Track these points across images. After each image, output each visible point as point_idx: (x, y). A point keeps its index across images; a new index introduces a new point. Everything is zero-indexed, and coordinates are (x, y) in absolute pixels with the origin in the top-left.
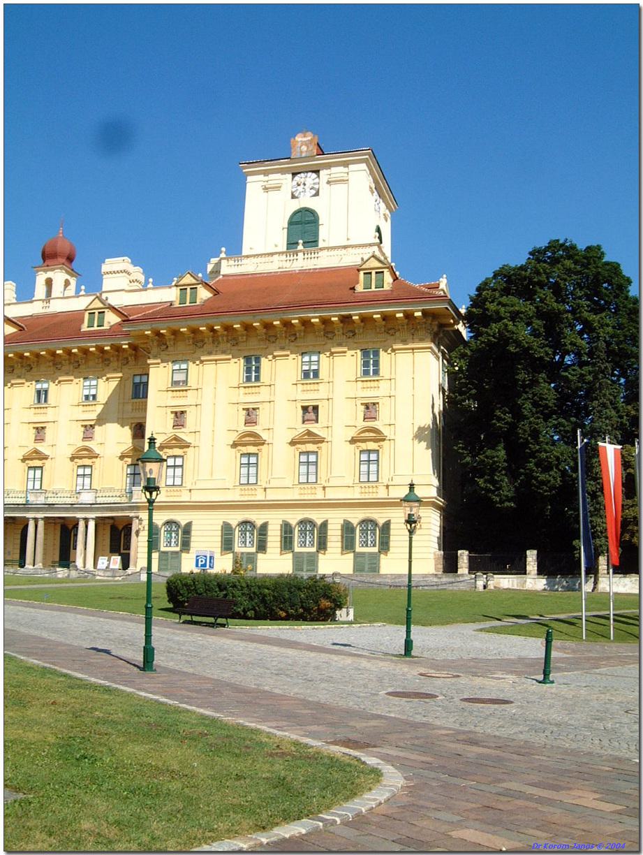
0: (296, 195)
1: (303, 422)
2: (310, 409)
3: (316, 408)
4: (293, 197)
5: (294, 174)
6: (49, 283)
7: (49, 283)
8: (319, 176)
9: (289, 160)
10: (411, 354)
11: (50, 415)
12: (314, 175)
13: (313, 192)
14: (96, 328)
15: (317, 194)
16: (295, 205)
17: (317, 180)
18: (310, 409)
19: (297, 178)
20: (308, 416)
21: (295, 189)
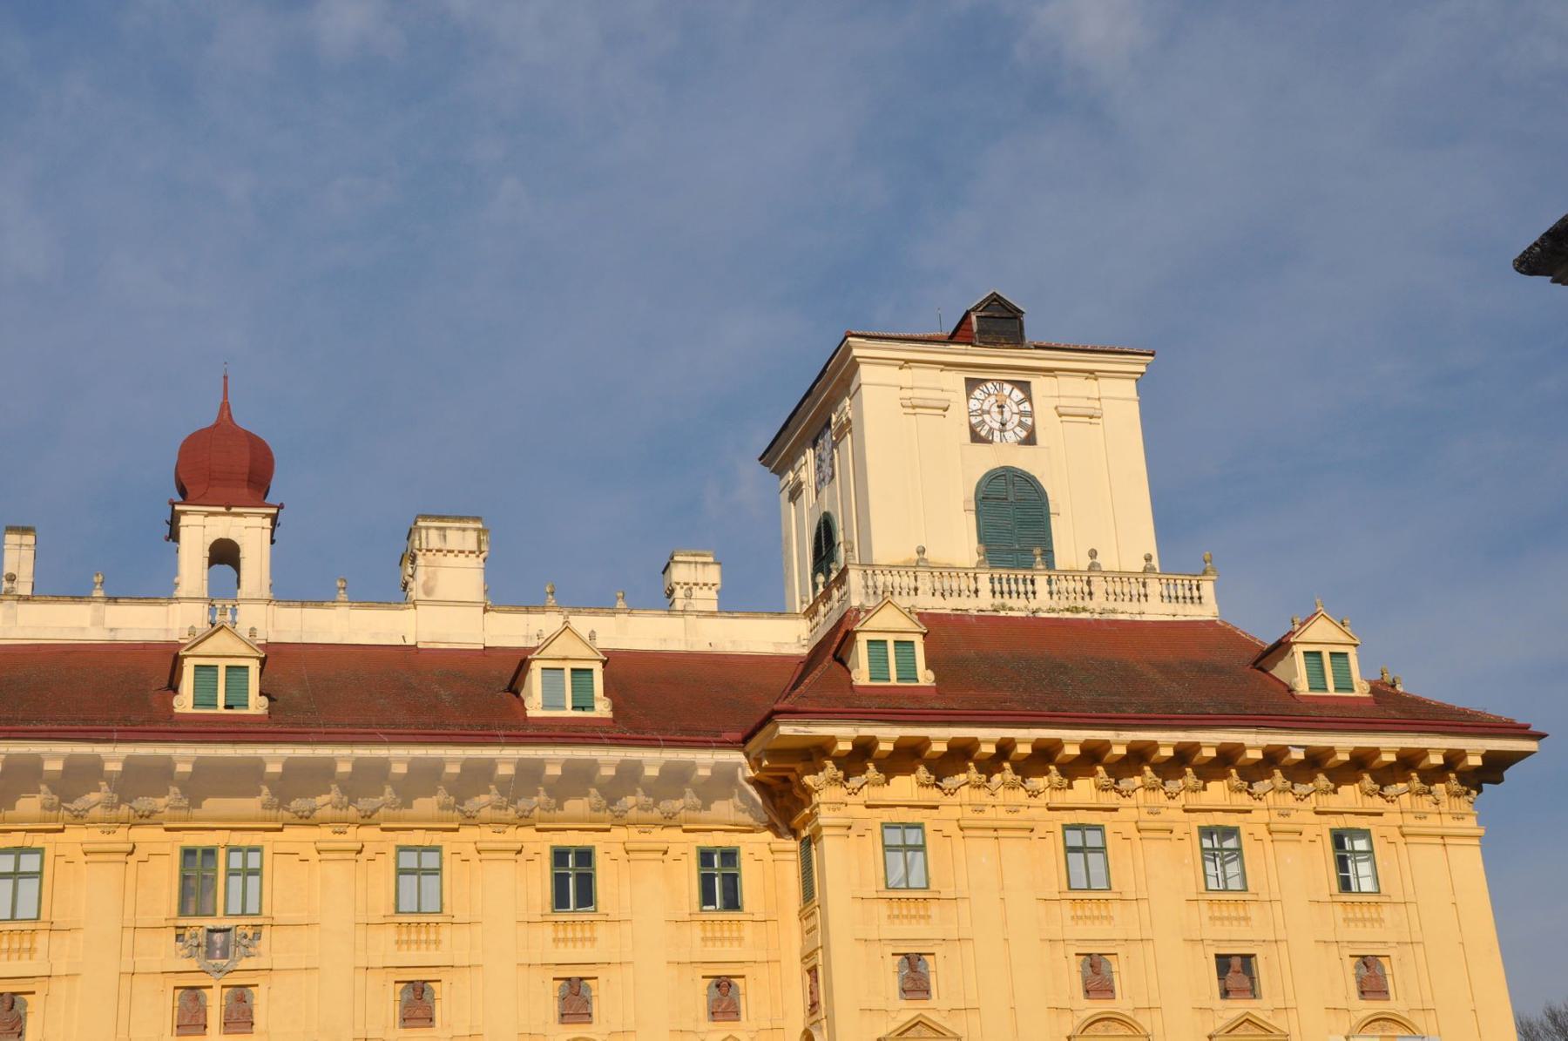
0: (983, 433)
1: (1225, 994)
2: (1236, 963)
3: (1247, 959)
4: (976, 437)
5: (972, 384)
6: (224, 554)
7: (224, 554)
8: (1028, 398)
9: (969, 347)
10: (1441, 848)
11: (450, 946)
12: (1018, 394)
13: (1023, 434)
14: (569, 713)
15: (1030, 440)
16: (987, 459)
17: (1026, 406)
18: (1236, 963)
19: (977, 393)
20: (1233, 980)
21: (979, 419)
